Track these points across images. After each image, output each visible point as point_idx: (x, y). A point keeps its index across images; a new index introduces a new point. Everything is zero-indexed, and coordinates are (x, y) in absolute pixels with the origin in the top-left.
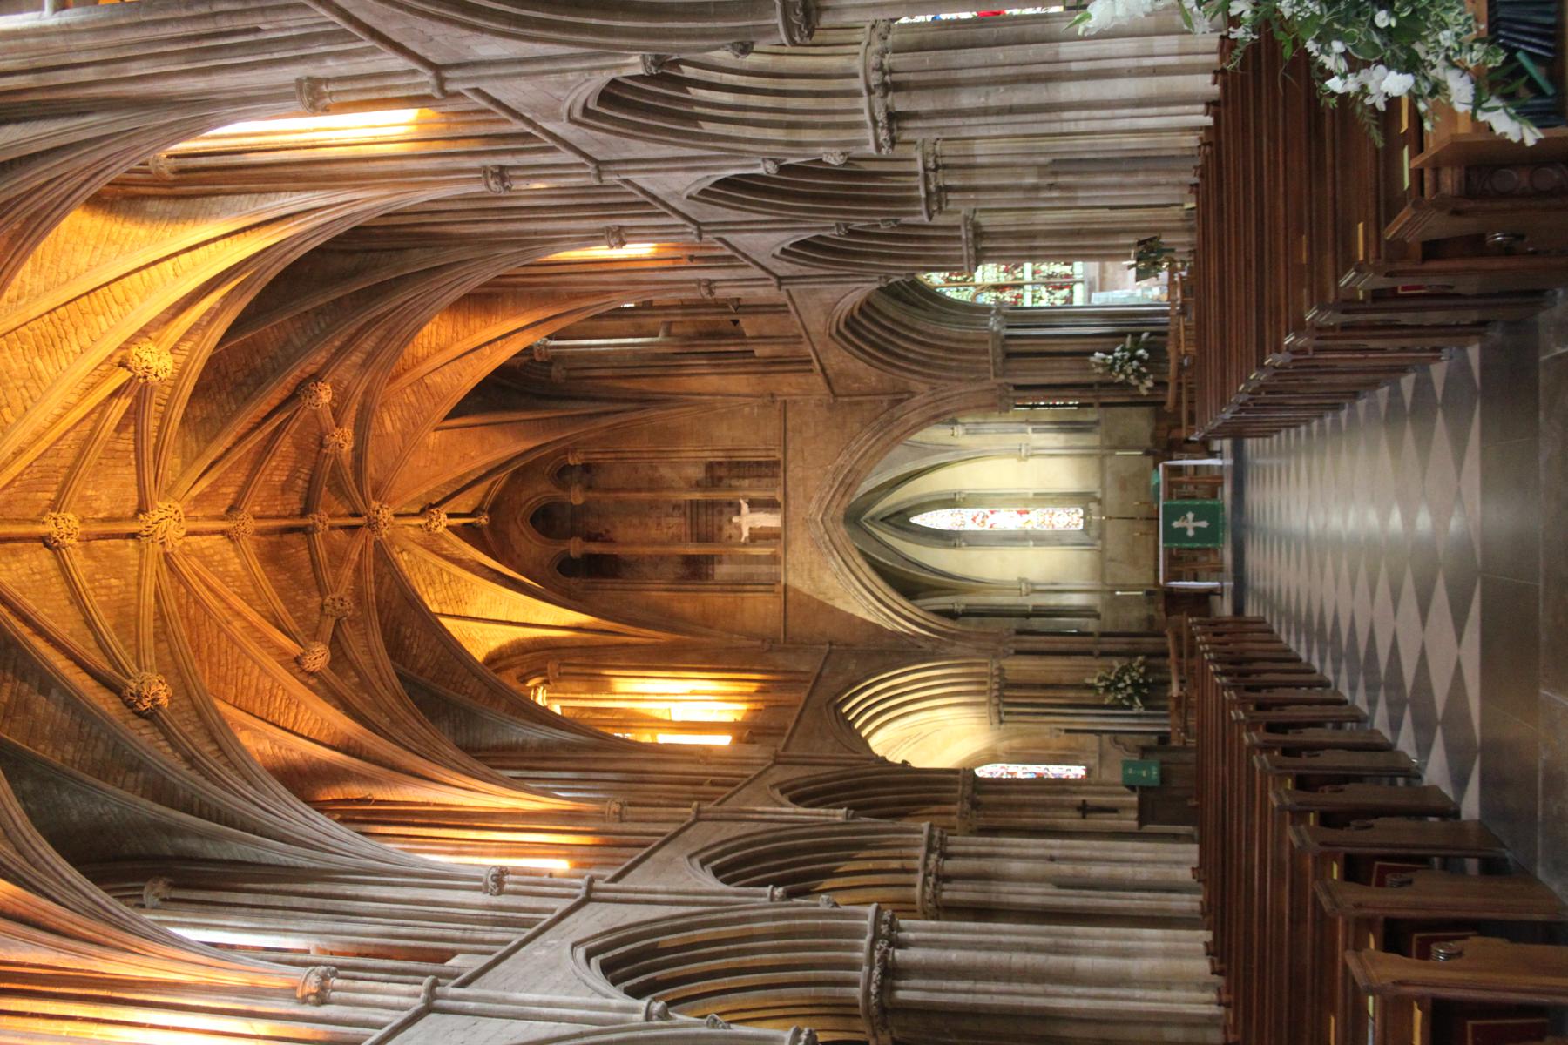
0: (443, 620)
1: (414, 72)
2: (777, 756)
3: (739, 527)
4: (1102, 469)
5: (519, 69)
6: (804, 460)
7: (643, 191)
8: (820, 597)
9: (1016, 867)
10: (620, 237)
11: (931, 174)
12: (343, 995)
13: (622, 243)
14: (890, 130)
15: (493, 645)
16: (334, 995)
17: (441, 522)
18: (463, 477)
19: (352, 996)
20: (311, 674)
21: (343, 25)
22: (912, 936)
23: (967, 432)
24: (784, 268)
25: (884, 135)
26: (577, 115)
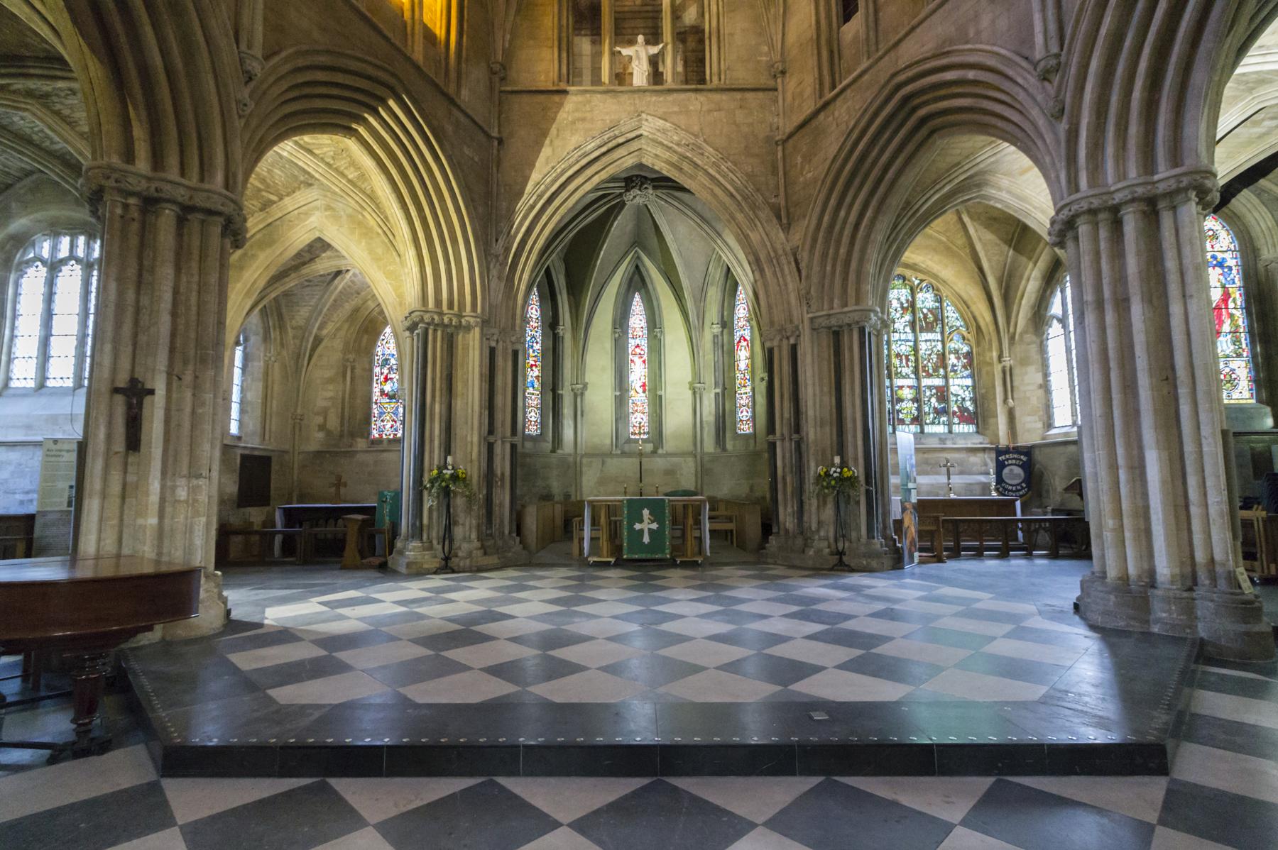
3: (632, 42)
4: (683, 454)
6: (709, 111)
8: (553, 131)
23: (715, 337)
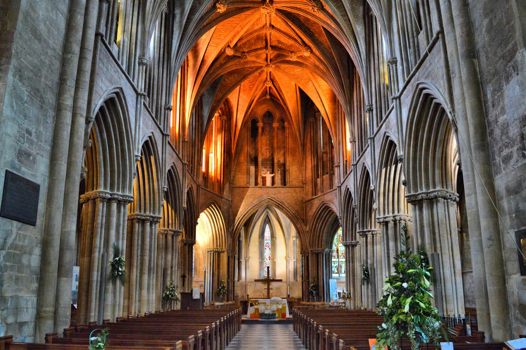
0: (239, 87)
1: (398, 91)
2: (199, 186)
3: (266, 173)
5: (399, 120)
7: (366, 150)
8: (245, 198)
9: (169, 257)
10: (353, 142)
11: (371, 233)
12: (141, 70)
13: (351, 142)
14: (383, 222)
15: (231, 100)
16: (141, 67)
17: (269, 84)
18: (281, 91)
19: (141, 72)
20: (225, 50)
21: (412, 73)
22: (153, 228)
23: (294, 241)
24: (343, 188)
25: (382, 220)
26: (387, 134)
